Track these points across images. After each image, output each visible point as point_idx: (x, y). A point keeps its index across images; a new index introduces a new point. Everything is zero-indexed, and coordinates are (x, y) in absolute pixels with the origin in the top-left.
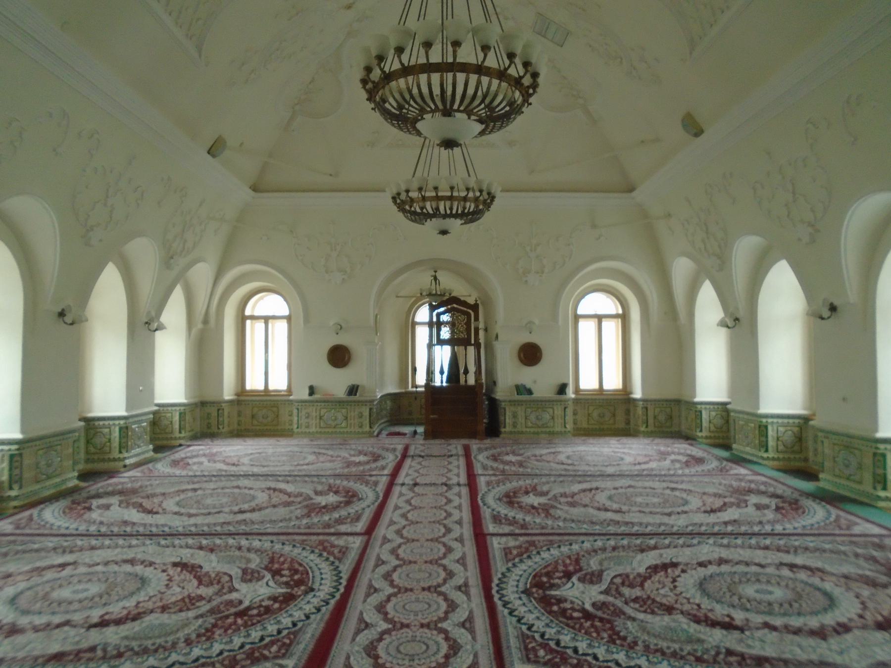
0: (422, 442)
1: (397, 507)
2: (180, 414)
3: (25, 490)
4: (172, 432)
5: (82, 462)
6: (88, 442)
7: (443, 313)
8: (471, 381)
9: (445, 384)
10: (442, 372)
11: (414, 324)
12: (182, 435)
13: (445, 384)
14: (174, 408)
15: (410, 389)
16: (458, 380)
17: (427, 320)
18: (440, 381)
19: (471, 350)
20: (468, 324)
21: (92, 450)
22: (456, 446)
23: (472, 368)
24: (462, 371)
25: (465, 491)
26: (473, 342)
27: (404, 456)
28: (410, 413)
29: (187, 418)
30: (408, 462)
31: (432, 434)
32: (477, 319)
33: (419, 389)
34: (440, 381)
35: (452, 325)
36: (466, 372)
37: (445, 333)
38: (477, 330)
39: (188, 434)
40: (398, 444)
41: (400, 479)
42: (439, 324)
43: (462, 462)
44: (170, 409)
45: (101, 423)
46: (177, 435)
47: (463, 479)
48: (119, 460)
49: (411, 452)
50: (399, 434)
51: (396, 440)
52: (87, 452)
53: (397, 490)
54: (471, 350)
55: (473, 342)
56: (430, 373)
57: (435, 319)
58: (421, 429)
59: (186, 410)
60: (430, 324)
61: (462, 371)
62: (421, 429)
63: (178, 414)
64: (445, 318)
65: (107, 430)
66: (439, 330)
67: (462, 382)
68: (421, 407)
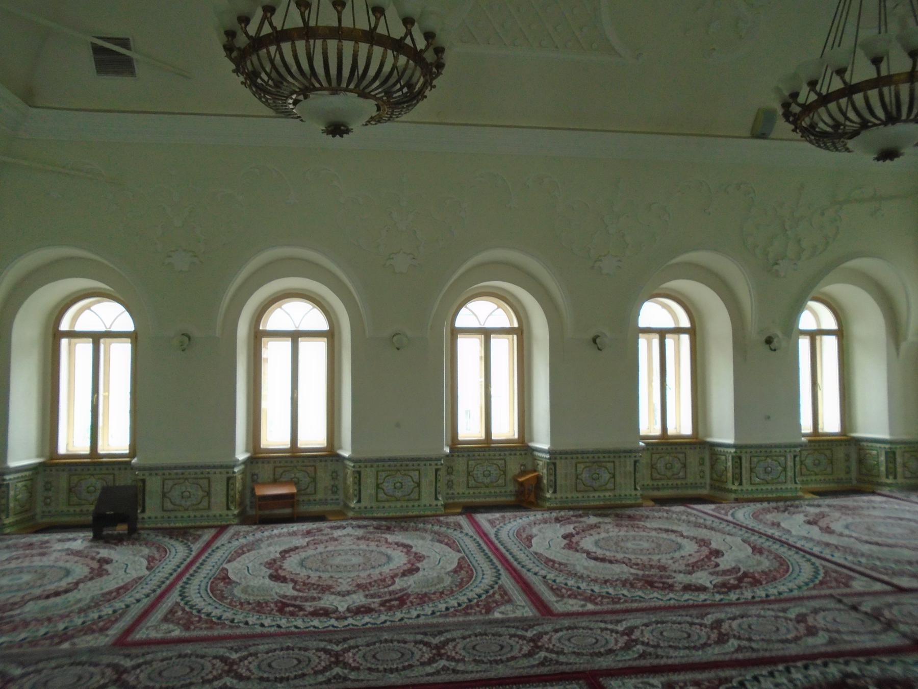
2: (886, 453)
3: (558, 495)
4: (878, 476)
5: (708, 487)
6: (712, 467)
12: (890, 481)
14: (878, 445)
21: (715, 476)
29: (899, 460)
39: (900, 480)
44: (874, 445)
45: (722, 449)
46: (884, 480)
48: (730, 491)
52: (712, 479)
59: (892, 449)
63: (883, 453)
65: (723, 458)
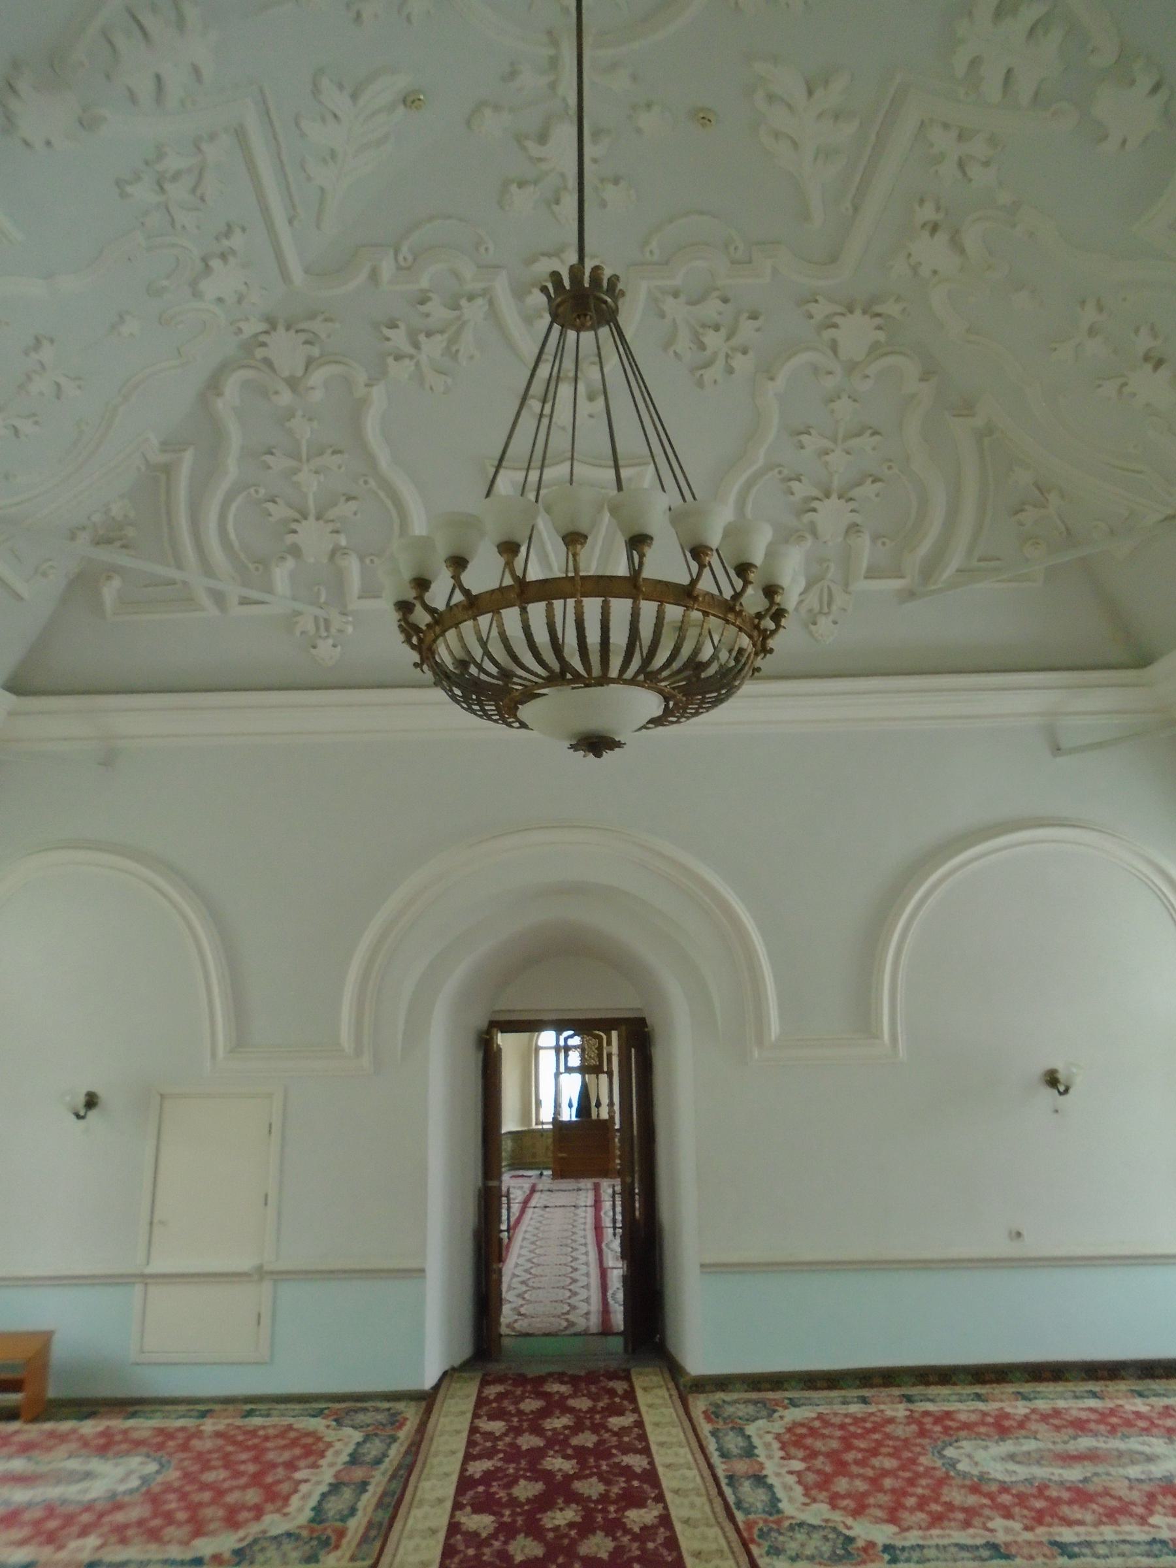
0: (550, 1181)
1: (514, 1275)
7: (571, 1037)
8: (604, 1115)
9: (574, 1119)
10: (570, 1106)
11: (538, 1049)
13: (574, 1119)
15: (534, 1126)
16: (589, 1115)
17: (554, 1044)
18: (568, 1115)
19: (604, 1078)
20: (600, 1048)
22: (587, 1183)
23: (605, 1101)
24: (593, 1103)
25: (591, 1211)
26: (605, 1069)
27: (533, 1190)
28: (534, 1155)
30: (537, 1195)
31: (561, 1173)
32: (609, 1043)
33: (545, 1127)
34: (568, 1115)
35: (582, 1049)
36: (598, 1105)
37: (575, 1059)
38: (609, 1056)
40: (527, 1185)
41: (533, 1203)
42: (567, 1049)
43: (591, 1194)
47: (590, 1201)
49: (540, 1187)
50: (523, 1176)
51: (520, 1180)
53: (529, 1212)
54: (604, 1078)
55: (605, 1069)
56: (557, 1106)
57: (562, 1043)
58: (550, 1172)
60: (557, 1049)
61: (593, 1103)
62: (550, 1172)
64: (576, 1041)
66: (566, 1056)
67: (594, 1116)
68: (547, 1148)
